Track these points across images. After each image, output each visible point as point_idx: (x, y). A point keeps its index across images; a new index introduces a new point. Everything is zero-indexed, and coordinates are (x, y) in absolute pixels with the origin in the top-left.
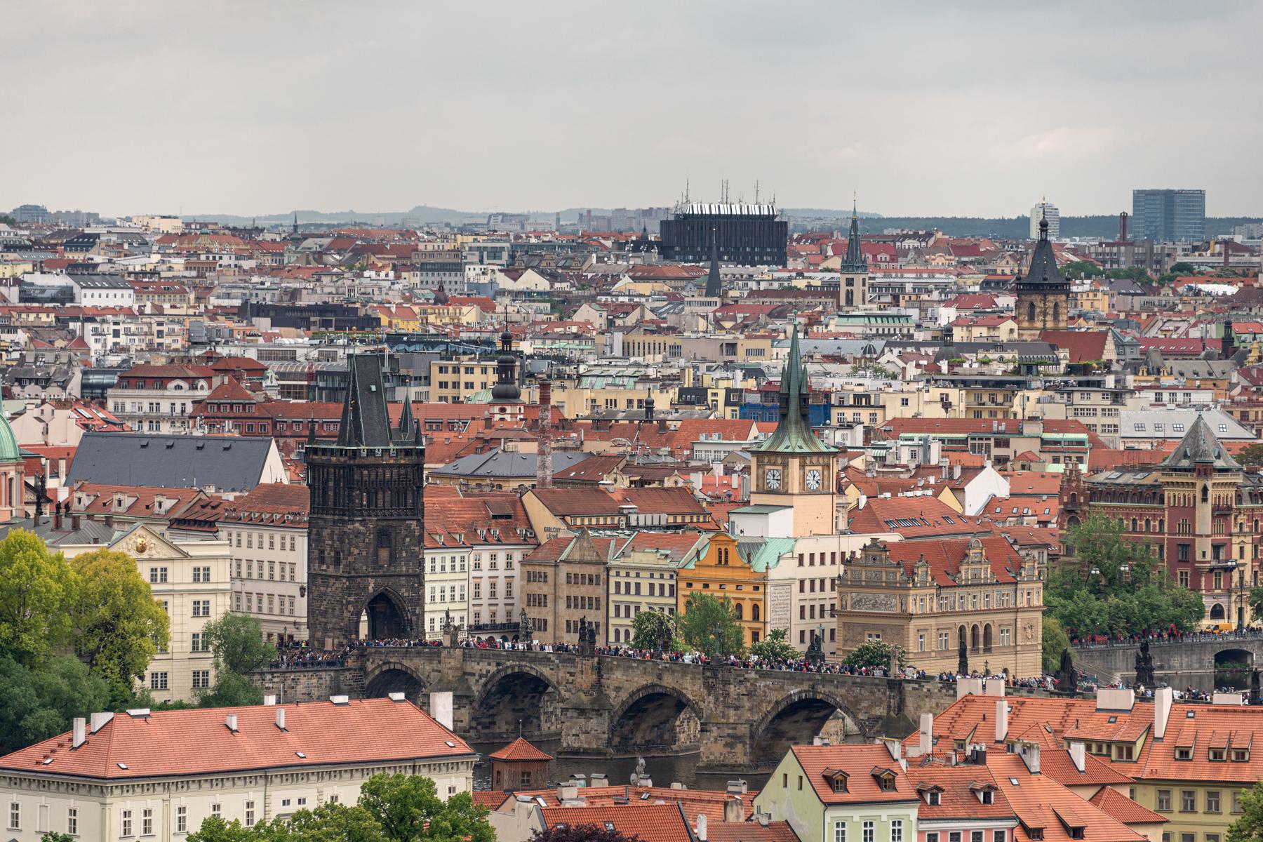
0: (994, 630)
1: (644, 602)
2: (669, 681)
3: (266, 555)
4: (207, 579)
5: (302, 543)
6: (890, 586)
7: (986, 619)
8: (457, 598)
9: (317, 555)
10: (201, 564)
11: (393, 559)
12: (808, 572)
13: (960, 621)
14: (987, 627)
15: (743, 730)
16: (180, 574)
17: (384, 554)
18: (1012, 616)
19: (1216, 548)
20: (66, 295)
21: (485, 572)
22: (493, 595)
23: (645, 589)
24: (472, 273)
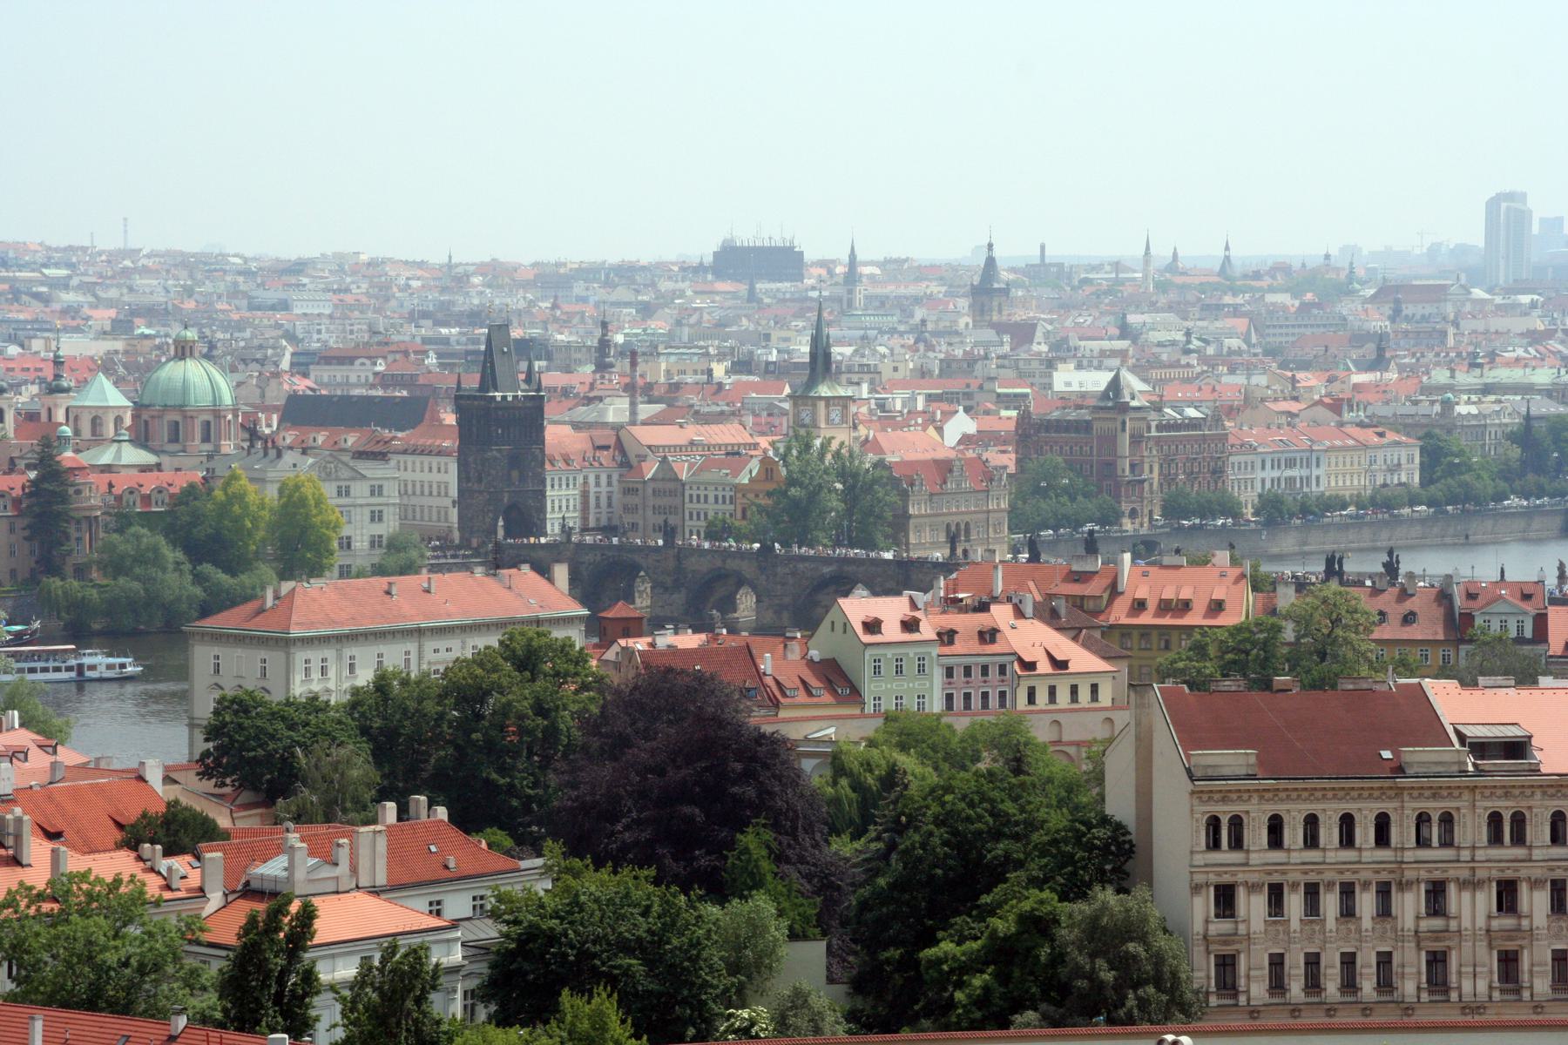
0: (972, 526)
1: (711, 509)
2: (732, 564)
3: (426, 477)
4: (380, 494)
5: (453, 468)
7: (967, 518)
8: (571, 508)
10: (376, 483)
11: (522, 478)
13: (948, 519)
14: (967, 524)
15: (787, 600)
17: (515, 474)
18: (985, 516)
19: (1132, 466)
22: (598, 506)
23: (711, 499)
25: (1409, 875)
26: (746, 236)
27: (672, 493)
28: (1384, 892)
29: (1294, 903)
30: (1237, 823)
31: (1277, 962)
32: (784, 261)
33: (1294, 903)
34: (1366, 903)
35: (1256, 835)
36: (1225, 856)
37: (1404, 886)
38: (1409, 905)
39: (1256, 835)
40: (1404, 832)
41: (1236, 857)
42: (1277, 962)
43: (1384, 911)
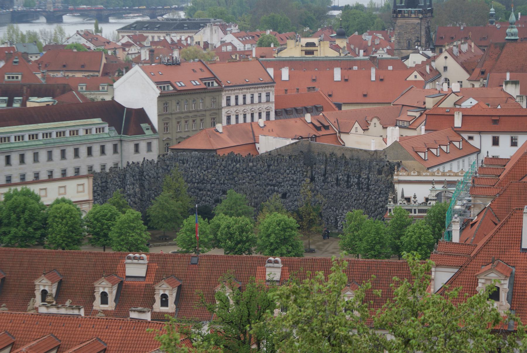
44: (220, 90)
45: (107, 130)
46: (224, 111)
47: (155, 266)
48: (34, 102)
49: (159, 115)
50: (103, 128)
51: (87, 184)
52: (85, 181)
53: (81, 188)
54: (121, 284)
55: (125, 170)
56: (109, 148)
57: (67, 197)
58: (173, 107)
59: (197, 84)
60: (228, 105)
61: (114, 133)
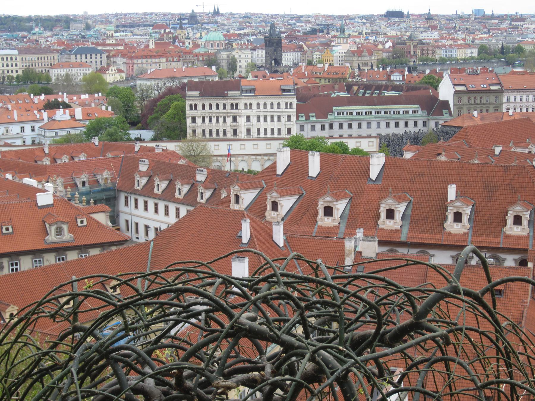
5: (264, 51)
6: (351, 56)
9: (266, 53)
12: (340, 55)
16: (243, 56)
20: (295, 24)
21: (297, 56)
24: (356, 20)
25: (229, 115)
26: (393, 8)
27: (311, 57)
28: (225, 118)
29: (207, 120)
30: (196, 106)
31: (204, 131)
32: (399, 14)
33: (207, 120)
34: (221, 120)
35: (199, 107)
36: (193, 111)
37: (228, 117)
38: (229, 120)
39: (199, 107)
40: (228, 107)
41: (196, 111)
42: (204, 131)
43: (225, 121)
44: (501, 92)
45: (420, 112)
46: (504, 106)
47: (211, 176)
48: (387, 94)
49: (454, 105)
50: (418, 111)
51: (376, 142)
52: (374, 140)
53: (371, 144)
54: (193, 185)
55: (403, 135)
56: (420, 123)
57: (361, 148)
58: (465, 100)
59: (484, 87)
60: (508, 100)
61: (425, 114)
